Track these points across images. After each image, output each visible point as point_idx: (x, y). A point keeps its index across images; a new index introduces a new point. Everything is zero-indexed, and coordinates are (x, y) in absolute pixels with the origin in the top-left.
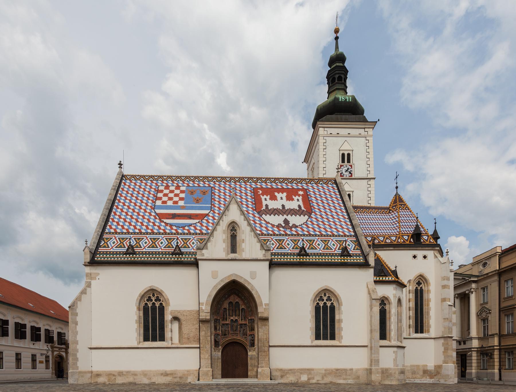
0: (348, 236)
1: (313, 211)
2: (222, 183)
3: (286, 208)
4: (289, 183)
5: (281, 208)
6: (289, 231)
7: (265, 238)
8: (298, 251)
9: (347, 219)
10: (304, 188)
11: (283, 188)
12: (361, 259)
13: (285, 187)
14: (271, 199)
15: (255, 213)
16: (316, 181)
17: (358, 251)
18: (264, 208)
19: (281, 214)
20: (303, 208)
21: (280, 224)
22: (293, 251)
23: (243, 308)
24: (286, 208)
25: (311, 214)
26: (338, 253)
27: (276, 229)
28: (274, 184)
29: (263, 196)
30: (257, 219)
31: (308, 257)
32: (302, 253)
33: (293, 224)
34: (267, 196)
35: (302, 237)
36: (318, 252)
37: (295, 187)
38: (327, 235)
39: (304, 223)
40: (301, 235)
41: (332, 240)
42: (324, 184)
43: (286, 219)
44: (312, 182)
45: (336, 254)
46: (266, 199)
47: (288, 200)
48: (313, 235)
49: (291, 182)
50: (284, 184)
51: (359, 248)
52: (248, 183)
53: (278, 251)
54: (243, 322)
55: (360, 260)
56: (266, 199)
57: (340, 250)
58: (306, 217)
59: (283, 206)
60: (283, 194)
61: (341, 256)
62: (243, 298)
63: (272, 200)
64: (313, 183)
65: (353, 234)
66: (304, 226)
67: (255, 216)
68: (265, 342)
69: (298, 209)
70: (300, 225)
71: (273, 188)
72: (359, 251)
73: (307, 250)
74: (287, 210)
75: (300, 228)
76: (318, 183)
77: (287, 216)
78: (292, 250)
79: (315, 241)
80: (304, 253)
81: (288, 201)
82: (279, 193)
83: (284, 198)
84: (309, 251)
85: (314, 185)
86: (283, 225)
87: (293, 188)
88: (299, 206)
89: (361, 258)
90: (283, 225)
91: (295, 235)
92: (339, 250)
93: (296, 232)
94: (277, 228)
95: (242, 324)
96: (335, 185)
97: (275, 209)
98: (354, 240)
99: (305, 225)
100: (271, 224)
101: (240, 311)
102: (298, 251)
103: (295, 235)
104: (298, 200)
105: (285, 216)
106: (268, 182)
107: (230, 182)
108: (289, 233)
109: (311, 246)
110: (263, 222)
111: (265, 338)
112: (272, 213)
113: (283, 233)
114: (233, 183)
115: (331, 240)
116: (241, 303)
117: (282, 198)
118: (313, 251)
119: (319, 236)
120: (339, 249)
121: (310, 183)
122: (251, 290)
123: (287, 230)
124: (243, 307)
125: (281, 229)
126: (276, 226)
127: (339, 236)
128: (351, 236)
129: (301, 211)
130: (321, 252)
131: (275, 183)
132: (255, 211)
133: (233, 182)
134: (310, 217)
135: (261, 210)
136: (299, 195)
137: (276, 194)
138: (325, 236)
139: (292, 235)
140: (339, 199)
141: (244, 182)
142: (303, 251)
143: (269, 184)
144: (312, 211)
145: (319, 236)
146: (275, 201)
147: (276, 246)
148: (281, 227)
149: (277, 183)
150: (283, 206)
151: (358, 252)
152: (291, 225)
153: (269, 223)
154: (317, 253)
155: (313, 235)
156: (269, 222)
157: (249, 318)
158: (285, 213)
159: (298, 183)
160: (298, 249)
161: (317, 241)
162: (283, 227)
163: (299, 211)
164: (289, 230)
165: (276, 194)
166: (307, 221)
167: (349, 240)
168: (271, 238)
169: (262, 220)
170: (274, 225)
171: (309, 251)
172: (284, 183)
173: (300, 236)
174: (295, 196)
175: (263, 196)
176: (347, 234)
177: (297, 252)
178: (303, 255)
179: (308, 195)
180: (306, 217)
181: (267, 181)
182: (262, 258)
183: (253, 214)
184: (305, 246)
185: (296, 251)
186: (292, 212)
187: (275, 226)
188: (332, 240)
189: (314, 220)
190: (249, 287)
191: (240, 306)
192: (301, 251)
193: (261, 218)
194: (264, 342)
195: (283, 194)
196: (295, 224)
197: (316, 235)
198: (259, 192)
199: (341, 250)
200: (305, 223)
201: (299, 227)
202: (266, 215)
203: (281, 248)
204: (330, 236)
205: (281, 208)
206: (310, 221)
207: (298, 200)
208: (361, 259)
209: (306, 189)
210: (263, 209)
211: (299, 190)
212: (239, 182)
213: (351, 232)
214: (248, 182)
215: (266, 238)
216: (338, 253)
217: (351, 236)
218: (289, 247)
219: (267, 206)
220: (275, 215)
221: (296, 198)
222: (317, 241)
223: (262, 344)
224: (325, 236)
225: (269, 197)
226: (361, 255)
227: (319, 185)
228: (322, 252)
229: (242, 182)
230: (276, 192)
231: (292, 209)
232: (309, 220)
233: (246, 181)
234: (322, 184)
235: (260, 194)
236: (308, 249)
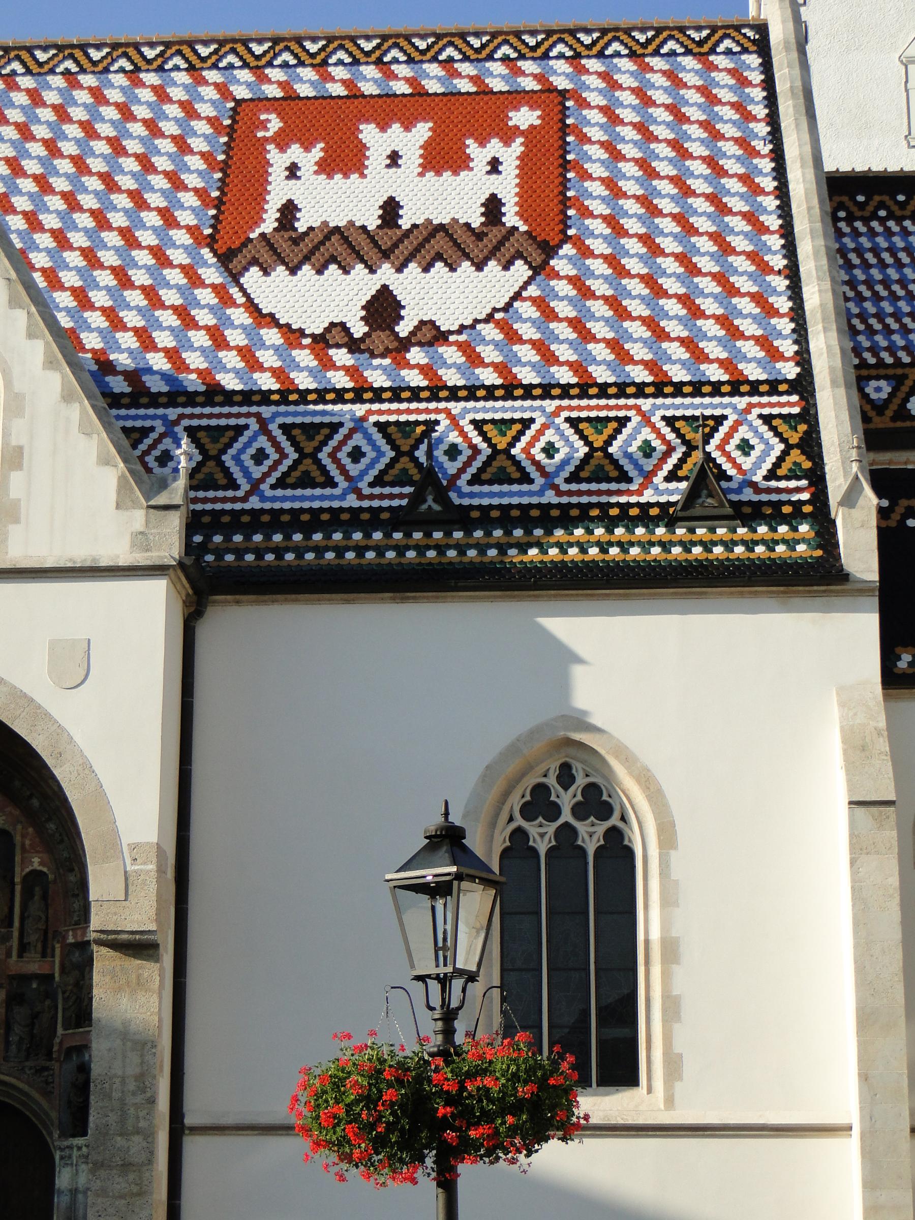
0: (755, 388)
1: (570, 232)
2: (57, 81)
3: (405, 223)
4: (466, 58)
5: (373, 223)
6: (384, 369)
7: (219, 416)
8: (401, 496)
9: (779, 272)
10: (550, 89)
11: (420, 93)
12: (803, 540)
13: (433, 87)
14: (326, 167)
15: (205, 264)
16: (642, 38)
17: (793, 484)
18: (269, 225)
19: (362, 260)
20: (511, 218)
21: (343, 325)
22: (371, 497)
23: (36, 875)
24: (405, 223)
25: (549, 250)
26: (663, 499)
27: (304, 357)
28: (370, 71)
29: (282, 148)
30: (206, 296)
31: (458, 535)
32: (424, 507)
33: (422, 323)
34: (307, 149)
35: (456, 407)
36: (535, 500)
37: (497, 85)
38: (621, 389)
39: (495, 310)
40: (454, 394)
41: (646, 420)
42: (688, 52)
43: (385, 287)
44: (616, 46)
45: (645, 507)
46: (293, 171)
47: (433, 168)
48: (528, 392)
49: (484, 55)
50: (433, 69)
51: (807, 465)
52: (212, 76)
53: (284, 499)
54: (33, 965)
55: (791, 544)
56: (293, 171)
57: (680, 480)
58: (520, 270)
59: (391, 209)
60: (407, 129)
61: (671, 525)
62: (35, 803)
63: (330, 176)
64: (617, 54)
65: (790, 371)
66: (489, 331)
67: (195, 280)
68: (130, 1100)
69: (477, 221)
70: (462, 329)
71: (355, 95)
72: (804, 483)
73: (467, 489)
74: (409, 231)
75: (460, 345)
76: (650, 49)
77: (399, 270)
78: (367, 491)
79: (535, 427)
80: (437, 507)
81: (430, 175)
82: (383, 128)
83: (412, 158)
84: (472, 495)
85: (625, 64)
86: (359, 329)
87: (485, 92)
88: (493, 206)
89: (804, 528)
90: (359, 329)
91: (415, 394)
92: (673, 485)
93: (426, 370)
94: (313, 350)
95: (26, 978)
96: (754, 60)
97: (337, 229)
98: (785, 411)
99: (498, 323)
100: (286, 329)
101: (18, 888)
102: (401, 496)
103: (415, 394)
104: (494, 166)
105: (386, 274)
106: (340, 62)
107: (106, 70)
108: (378, 379)
109: (501, 460)
110: (240, 316)
111: (132, 1070)
112: (306, 259)
113: (341, 380)
114: (120, 80)
115: (636, 419)
116: (23, 835)
117: (394, 159)
118: (501, 495)
119: (565, 391)
120: (672, 477)
121: (601, 55)
122: (49, 762)
123: (376, 362)
124: (36, 863)
125: (341, 356)
126: (313, 336)
127: (697, 388)
128: (773, 387)
129: (495, 234)
130: (550, 497)
131: (379, 62)
132: (206, 253)
133: (122, 70)
134: (540, 269)
135: (251, 240)
136: (508, 135)
137: (368, 133)
138: (603, 390)
139: (396, 393)
140: (758, 145)
141: (191, 69)
142: (430, 499)
143: (339, 72)
144: (564, 232)
145: (565, 391)
146: (346, 176)
147: (273, 468)
148: (338, 346)
149: (396, 61)
150: (391, 209)
151: (798, 490)
152: (403, 329)
153: (272, 320)
154: (525, 509)
155: (528, 392)
156: (272, 315)
157: (71, 940)
158: (386, 255)
159: (522, 57)
160: (411, 483)
161: (545, 427)
162: (353, 345)
163: (479, 236)
164: (387, 361)
165: (368, 133)
166: (517, 296)
167: (756, 411)
168: (258, 415)
169: (234, 304)
170: (301, 333)
171: (472, 495)
172: (434, 59)
173: (447, 399)
174: (482, 143)
175: (282, 148)
176: (754, 372)
177: (396, 503)
178: (428, 523)
179: (564, 130)
180: (520, 270)
181: (334, 52)
182: (125, 559)
183: (189, 271)
184: (452, 468)
185: (391, 497)
186: (440, 243)
187: (307, 341)
188: (646, 420)
189: (563, 288)
190: (38, 742)
191: (18, 858)
192: (417, 499)
193: (234, 291)
194: (122, 1101)
195: (407, 129)
196: (432, 323)
197: (546, 391)
198: (264, 125)
199: (684, 485)
200: (498, 316)
201: (452, 338)
202: (266, 272)
203: (306, 481)
204: (640, 390)
205: (373, 223)
206: (534, 300)
207: (494, 166)
208: (803, 540)
209: (564, 94)
210: (263, 235)
211: (517, 97)
212: (160, 69)
213: (781, 357)
214: (215, 66)
215: (229, 416)
216: (657, 504)
217: (773, 387)
218: (352, 473)
219: (289, 210)
220: (320, 272)
221: (479, 155)
222: (545, 427)
223: (113, 1118)
224: (603, 390)
225: (317, 152)
226: (807, 509)
227: (657, 63)
228: (555, 500)
229: (177, 68)
230: (367, 121)
231: (441, 227)
232: (533, 291)
233: (203, 60)
234: (673, 53)
235: (266, 140)
236: (475, 480)
